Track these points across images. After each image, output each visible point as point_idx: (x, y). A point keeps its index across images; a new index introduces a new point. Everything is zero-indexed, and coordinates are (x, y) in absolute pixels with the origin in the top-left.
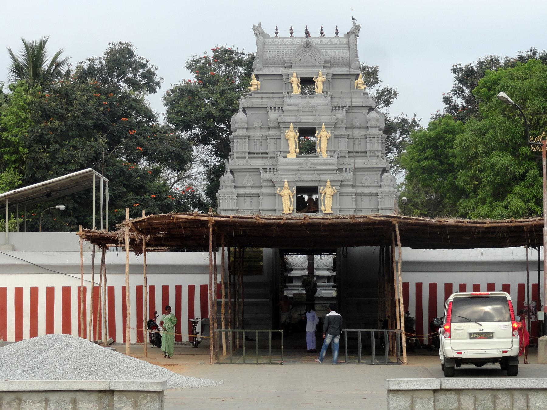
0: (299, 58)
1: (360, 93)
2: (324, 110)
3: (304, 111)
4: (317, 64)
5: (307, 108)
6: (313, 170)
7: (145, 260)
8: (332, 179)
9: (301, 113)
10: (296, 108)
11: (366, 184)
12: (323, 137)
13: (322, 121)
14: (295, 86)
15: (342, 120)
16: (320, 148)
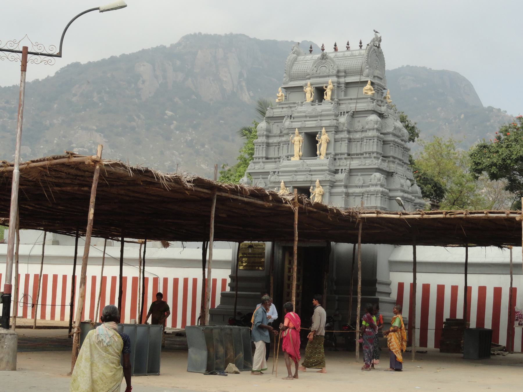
0: (315, 69)
1: (367, 98)
2: (327, 115)
3: (310, 117)
4: (331, 73)
5: (314, 114)
6: (307, 171)
7: (43, 252)
8: (321, 179)
9: (308, 119)
10: (304, 114)
11: (359, 184)
12: (323, 139)
13: (323, 125)
14: (308, 95)
15: (344, 124)
16: (320, 151)
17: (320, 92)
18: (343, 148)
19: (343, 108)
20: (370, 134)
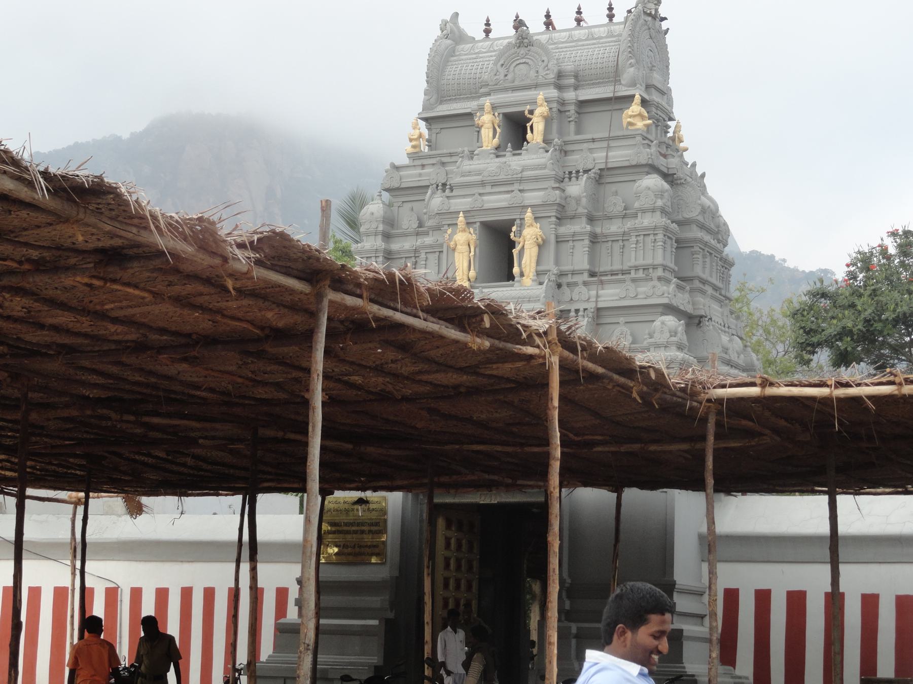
0: (502, 71)
1: (633, 137)
2: (537, 179)
3: (494, 184)
4: (541, 80)
5: (502, 177)
9: (488, 189)
10: (479, 178)
12: (528, 237)
13: (527, 203)
14: (486, 133)
15: (578, 200)
16: (520, 265)
17: (516, 128)
18: (579, 258)
19: (577, 160)
20: (646, 221)
